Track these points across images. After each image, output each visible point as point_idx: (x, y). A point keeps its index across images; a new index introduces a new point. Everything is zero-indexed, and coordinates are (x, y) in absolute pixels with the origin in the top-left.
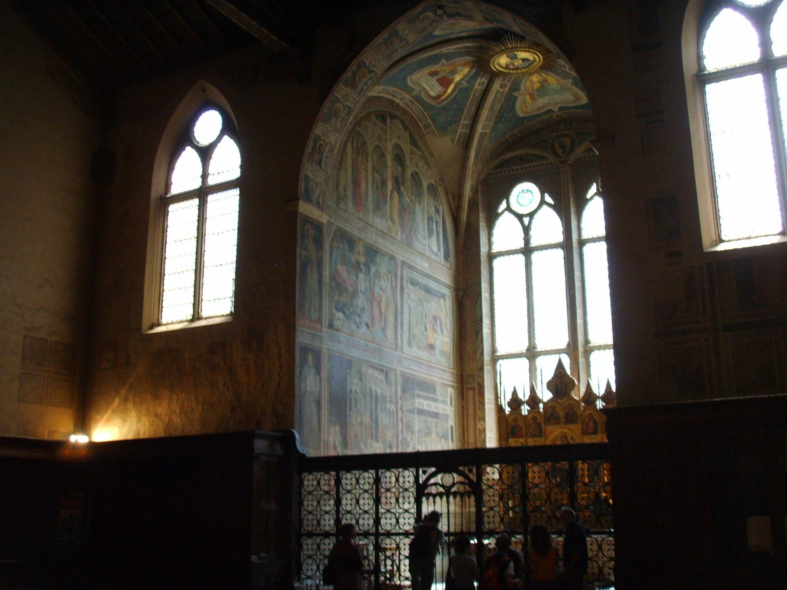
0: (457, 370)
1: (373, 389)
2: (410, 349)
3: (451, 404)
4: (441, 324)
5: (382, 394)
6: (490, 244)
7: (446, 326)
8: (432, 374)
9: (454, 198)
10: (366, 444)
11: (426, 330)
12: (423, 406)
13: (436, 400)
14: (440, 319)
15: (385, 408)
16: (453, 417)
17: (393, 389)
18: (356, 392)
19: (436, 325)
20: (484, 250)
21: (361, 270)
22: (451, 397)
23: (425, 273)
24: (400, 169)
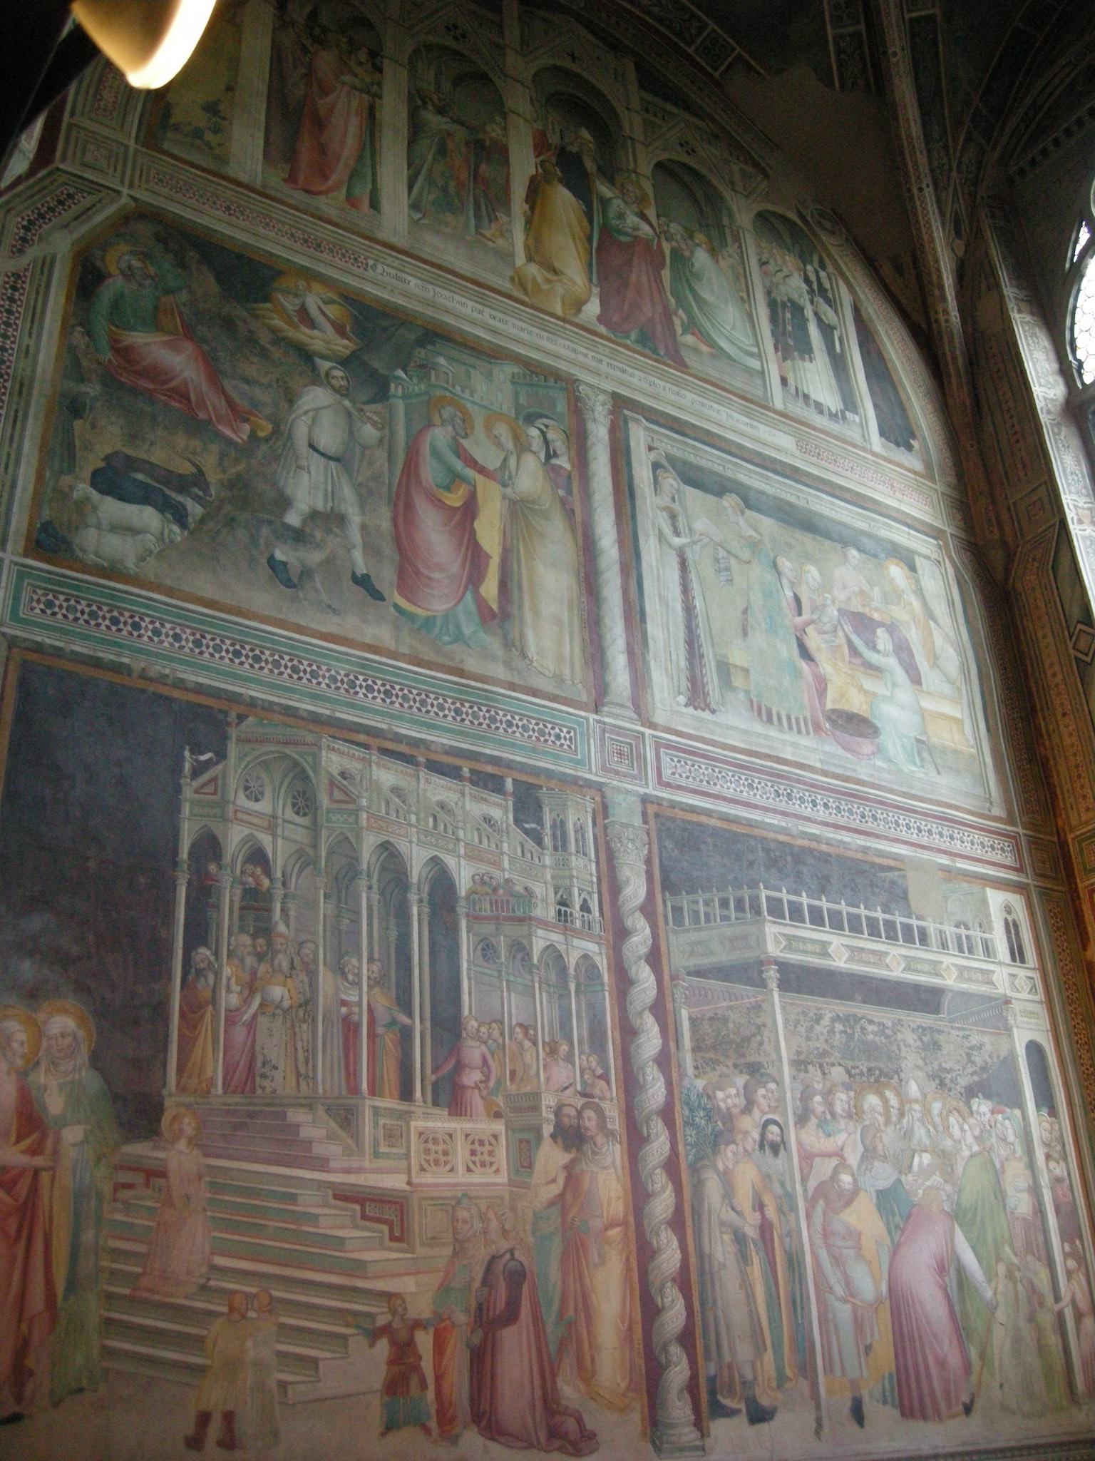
1: (417, 859)
2: (706, 715)
3: (1017, 954)
4: (903, 650)
5: (481, 881)
7: (934, 659)
8: (870, 826)
9: (898, 268)
10: (346, 1118)
12: (825, 954)
14: (892, 628)
15: (520, 949)
16: (1042, 1011)
17: (584, 868)
18: (258, 857)
19: (874, 648)
21: (316, 379)
22: (1012, 929)
23: (774, 460)
24: (585, 134)
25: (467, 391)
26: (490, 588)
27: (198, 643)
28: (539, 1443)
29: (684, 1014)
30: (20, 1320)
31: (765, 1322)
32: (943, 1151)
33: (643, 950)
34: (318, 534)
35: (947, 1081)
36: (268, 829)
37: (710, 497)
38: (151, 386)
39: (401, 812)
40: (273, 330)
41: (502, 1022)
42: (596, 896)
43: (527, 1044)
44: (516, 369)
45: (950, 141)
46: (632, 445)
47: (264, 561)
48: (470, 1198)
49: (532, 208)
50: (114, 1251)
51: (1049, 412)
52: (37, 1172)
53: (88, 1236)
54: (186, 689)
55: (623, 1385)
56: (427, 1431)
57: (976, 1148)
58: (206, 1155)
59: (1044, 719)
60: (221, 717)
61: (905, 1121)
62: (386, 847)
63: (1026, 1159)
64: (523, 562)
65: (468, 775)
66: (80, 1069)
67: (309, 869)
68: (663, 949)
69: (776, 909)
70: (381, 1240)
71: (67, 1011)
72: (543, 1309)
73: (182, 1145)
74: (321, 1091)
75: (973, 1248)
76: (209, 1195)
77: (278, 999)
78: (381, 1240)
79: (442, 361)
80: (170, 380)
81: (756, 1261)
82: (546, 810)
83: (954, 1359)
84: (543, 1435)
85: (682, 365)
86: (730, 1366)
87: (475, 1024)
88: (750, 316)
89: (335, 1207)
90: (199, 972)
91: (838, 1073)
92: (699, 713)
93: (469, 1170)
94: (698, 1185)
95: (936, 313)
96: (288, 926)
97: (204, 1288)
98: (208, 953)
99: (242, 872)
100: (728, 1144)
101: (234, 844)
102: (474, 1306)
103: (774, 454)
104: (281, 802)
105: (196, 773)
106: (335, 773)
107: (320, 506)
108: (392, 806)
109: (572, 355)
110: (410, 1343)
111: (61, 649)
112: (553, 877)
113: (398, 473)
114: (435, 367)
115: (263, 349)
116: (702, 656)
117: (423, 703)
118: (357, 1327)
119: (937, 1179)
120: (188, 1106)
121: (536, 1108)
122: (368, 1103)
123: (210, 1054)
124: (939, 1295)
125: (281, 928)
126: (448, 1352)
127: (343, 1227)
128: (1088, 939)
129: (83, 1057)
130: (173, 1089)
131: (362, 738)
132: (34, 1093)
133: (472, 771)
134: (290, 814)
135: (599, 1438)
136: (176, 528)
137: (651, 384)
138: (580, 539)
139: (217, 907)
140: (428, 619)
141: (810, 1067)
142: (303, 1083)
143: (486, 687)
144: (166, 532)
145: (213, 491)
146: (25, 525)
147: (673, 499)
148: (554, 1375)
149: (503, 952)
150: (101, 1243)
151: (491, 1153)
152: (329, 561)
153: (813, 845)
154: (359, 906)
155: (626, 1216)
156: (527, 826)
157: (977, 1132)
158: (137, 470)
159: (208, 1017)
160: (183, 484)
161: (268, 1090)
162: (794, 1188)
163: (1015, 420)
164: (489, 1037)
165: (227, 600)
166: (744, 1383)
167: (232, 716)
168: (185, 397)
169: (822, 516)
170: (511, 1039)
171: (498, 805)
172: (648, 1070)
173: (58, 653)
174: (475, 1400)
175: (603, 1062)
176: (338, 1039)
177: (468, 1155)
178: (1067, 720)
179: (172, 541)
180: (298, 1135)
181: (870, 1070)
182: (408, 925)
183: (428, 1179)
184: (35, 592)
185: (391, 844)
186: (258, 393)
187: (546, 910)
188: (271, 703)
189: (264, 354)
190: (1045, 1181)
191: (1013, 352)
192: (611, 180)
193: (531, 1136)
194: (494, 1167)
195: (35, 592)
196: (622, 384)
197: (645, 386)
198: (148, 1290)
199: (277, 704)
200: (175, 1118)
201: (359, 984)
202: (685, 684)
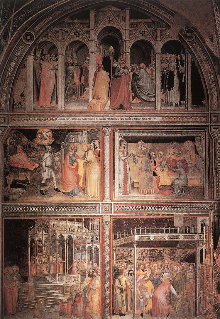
1: (66, 236)
2: (127, 196)
11: (155, 174)
15: (84, 248)
18: (40, 241)
21: (47, 151)
25: (77, 141)
26: (81, 183)
34: (48, 183)
42: (99, 236)
43: (84, 262)
49: (95, 83)
60: (34, 220)
69: (138, 232)
75: (175, 290)
81: (124, 292)
87: (75, 260)
92: (125, 196)
94: (114, 283)
105: (30, 230)
106: (52, 225)
107: (48, 178)
112: (91, 234)
121: (85, 272)
127: (54, 291)
131: (57, 218)
133: (76, 219)
134: (45, 233)
140: (69, 192)
147: (124, 148)
175: (98, 264)
187: (89, 239)
189: (36, 150)
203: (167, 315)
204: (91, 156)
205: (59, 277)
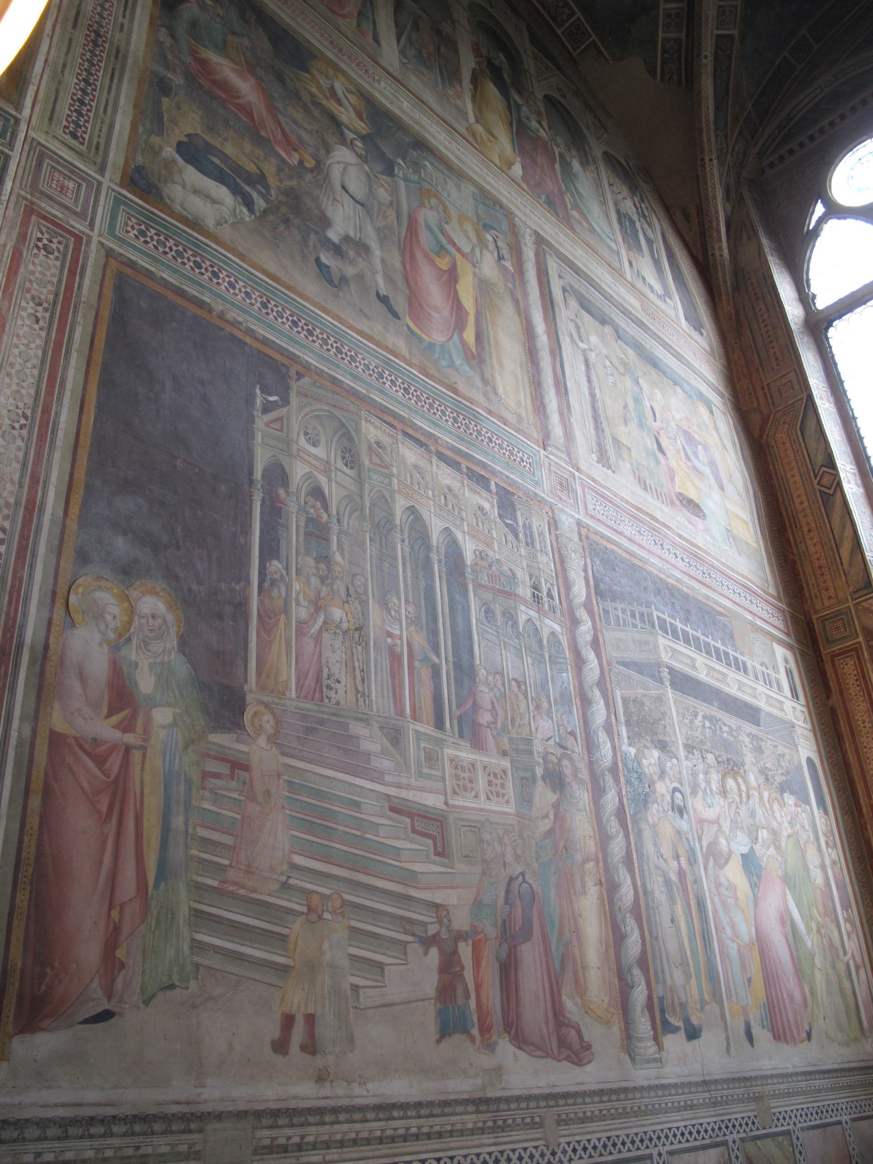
0: (789, 605)
1: (436, 526)
2: (609, 472)
5: (481, 556)
6: (805, 298)
8: (707, 581)
9: (687, 217)
13: (741, 667)
14: (706, 448)
15: (511, 617)
16: (810, 735)
17: (546, 563)
18: (317, 493)
20: (793, 312)
21: (343, 142)
22: (789, 673)
23: (630, 313)
26: (469, 335)
27: (264, 305)
28: (553, 1053)
29: (618, 694)
30: (110, 909)
31: (688, 953)
32: (773, 829)
33: (589, 638)
34: (352, 254)
35: (770, 777)
36: (325, 472)
37: (597, 323)
38: (223, 96)
39: (421, 486)
40: (312, 95)
41: (503, 675)
42: (556, 587)
43: (521, 697)
44: (475, 191)
45: (729, 132)
46: (549, 270)
47: (312, 260)
48: (491, 823)
50: (204, 840)
51: (796, 324)
52: (128, 749)
53: (178, 822)
54: (256, 339)
55: (606, 1000)
56: (473, 1040)
57: (790, 831)
58: (284, 754)
59: (793, 533)
61: (750, 802)
62: (412, 510)
63: (816, 844)
64: (490, 327)
65: (465, 470)
66: (170, 653)
67: (357, 514)
68: (601, 640)
70: (427, 857)
71: (157, 594)
72: (549, 929)
73: (262, 741)
74: (375, 710)
76: (287, 794)
77: (339, 620)
78: (427, 857)
79: (427, 164)
80: (238, 97)
81: (679, 902)
82: (519, 513)
83: (797, 995)
84: (555, 1044)
85: (572, 229)
86: (671, 988)
87: (484, 672)
88: (607, 215)
89: (390, 818)
90: (273, 583)
91: (710, 757)
93: (488, 798)
94: (639, 834)
95: (714, 249)
96: (343, 558)
97: (285, 886)
98: (280, 566)
99: (305, 503)
100: (653, 803)
101: (298, 478)
102: (500, 922)
103: (630, 308)
104: (333, 453)
106: (373, 441)
107: (352, 234)
108: (415, 481)
109: (508, 195)
110: (455, 952)
111: (152, 272)
112: (528, 566)
113: (404, 231)
114: (424, 167)
115: (305, 104)
116: (603, 431)
117: (431, 405)
118: (413, 935)
119: (772, 851)
120: (266, 705)
122: (412, 726)
123: (284, 659)
124: (784, 941)
125: (338, 558)
126: (484, 964)
127: (398, 839)
128: (831, 691)
129: (172, 642)
130: (254, 686)
131: (390, 419)
132: (125, 670)
134: (340, 464)
135: (593, 1050)
136: (245, 210)
137: (557, 234)
138: (524, 322)
139: (287, 527)
141: (694, 751)
142: (361, 700)
143: (473, 407)
144: (238, 211)
145: (273, 192)
146: (121, 161)
148: (559, 991)
149: (499, 617)
150: (191, 831)
151: (502, 785)
152: (360, 277)
153: (678, 585)
154: (396, 554)
155: (596, 853)
156: (507, 521)
157: (789, 819)
158: (215, 156)
159: (282, 625)
160: (250, 179)
161: (334, 701)
162: (695, 845)
163: (770, 327)
164: (495, 685)
165: (285, 278)
166: (681, 1004)
167: (293, 372)
168: (250, 115)
169: (661, 361)
170: (510, 691)
171: (487, 499)
172: (600, 734)
173: (150, 275)
174: (505, 1011)
176: (386, 663)
177: (487, 784)
178: (812, 534)
179: (242, 218)
180: (358, 747)
181: (728, 760)
182: (432, 578)
183: (459, 802)
184: (129, 219)
185: (416, 509)
186: (305, 136)
187: (525, 591)
188: (323, 371)
190: (828, 862)
191: (769, 282)
192: (520, 92)
193: (528, 775)
194: (506, 798)
195: (129, 219)
196: (539, 226)
197: (553, 234)
198: (235, 884)
199: (326, 373)
200: (255, 714)
201: (400, 621)
202: (595, 447)
203: (807, 1032)
204: (489, 267)
205: (419, 748)
